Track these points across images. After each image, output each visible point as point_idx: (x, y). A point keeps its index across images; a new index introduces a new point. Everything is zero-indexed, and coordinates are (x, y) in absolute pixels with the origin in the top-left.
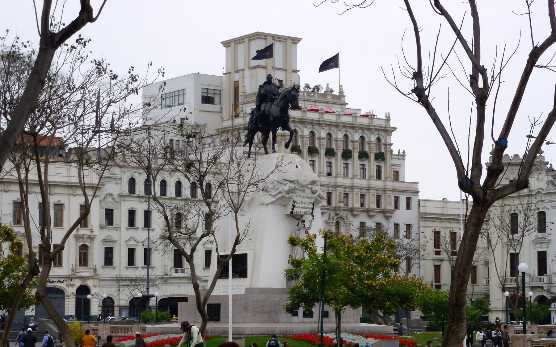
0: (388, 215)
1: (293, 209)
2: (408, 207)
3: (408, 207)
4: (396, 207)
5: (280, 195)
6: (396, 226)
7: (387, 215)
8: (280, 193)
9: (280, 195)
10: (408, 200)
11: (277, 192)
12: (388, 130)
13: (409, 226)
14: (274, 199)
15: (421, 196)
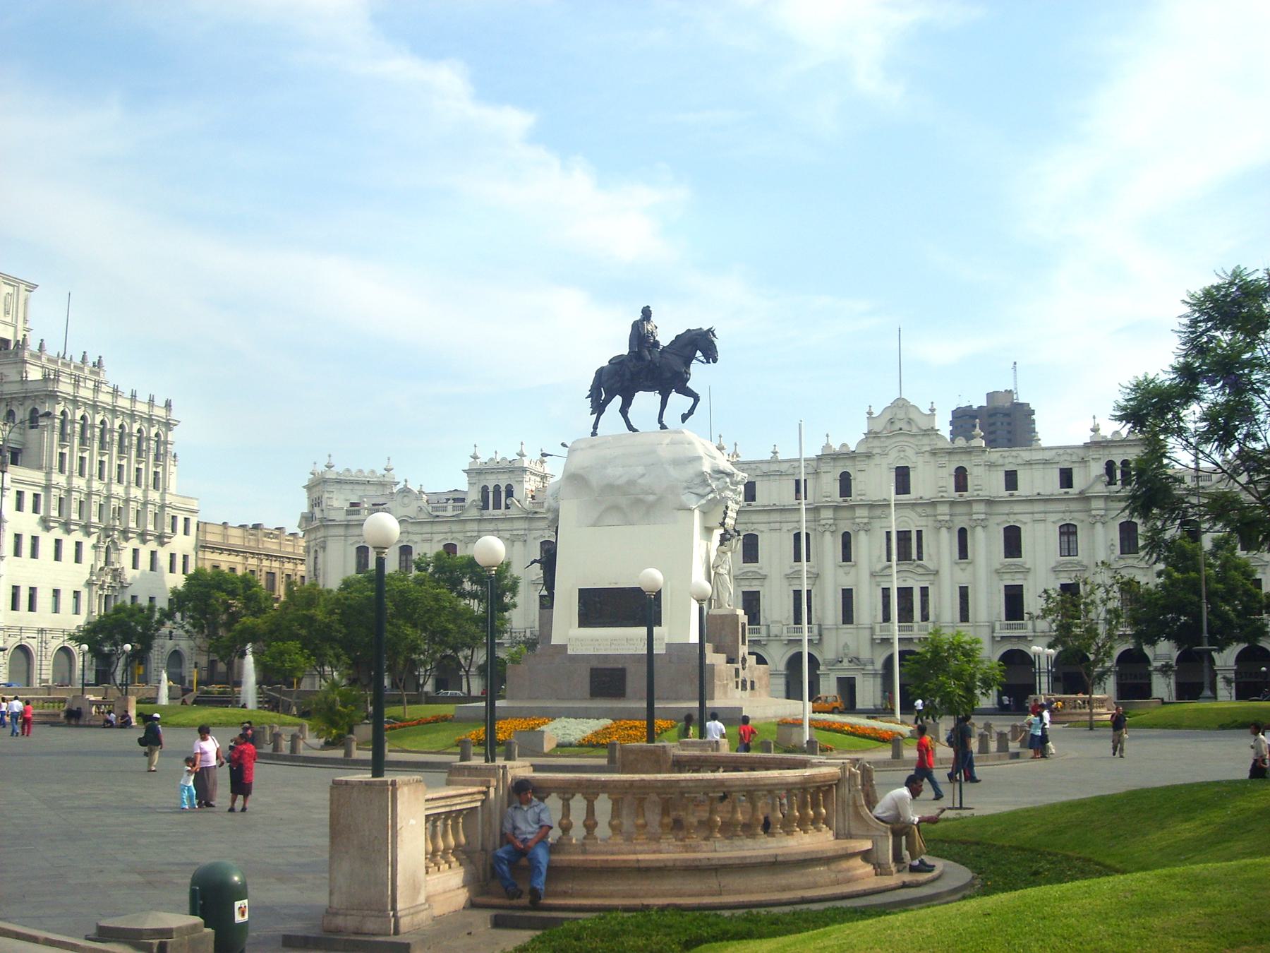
0: (166, 540)
1: (724, 519)
2: (186, 532)
3: (186, 532)
4: (174, 529)
5: (712, 495)
6: (172, 556)
7: (161, 540)
8: (712, 491)
9: (712, 495)
10: (186, 520)
11: (709, 489)
12: (168, 425)
13: (185, 557)
14: (703, 501)
15: (202, 517)
